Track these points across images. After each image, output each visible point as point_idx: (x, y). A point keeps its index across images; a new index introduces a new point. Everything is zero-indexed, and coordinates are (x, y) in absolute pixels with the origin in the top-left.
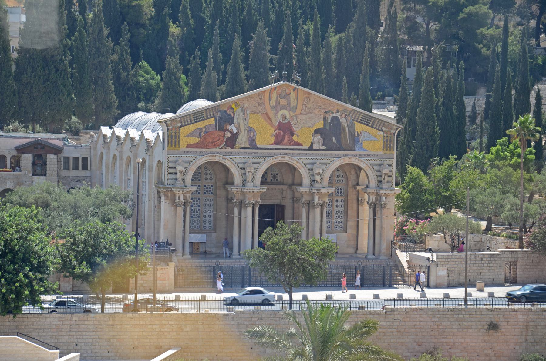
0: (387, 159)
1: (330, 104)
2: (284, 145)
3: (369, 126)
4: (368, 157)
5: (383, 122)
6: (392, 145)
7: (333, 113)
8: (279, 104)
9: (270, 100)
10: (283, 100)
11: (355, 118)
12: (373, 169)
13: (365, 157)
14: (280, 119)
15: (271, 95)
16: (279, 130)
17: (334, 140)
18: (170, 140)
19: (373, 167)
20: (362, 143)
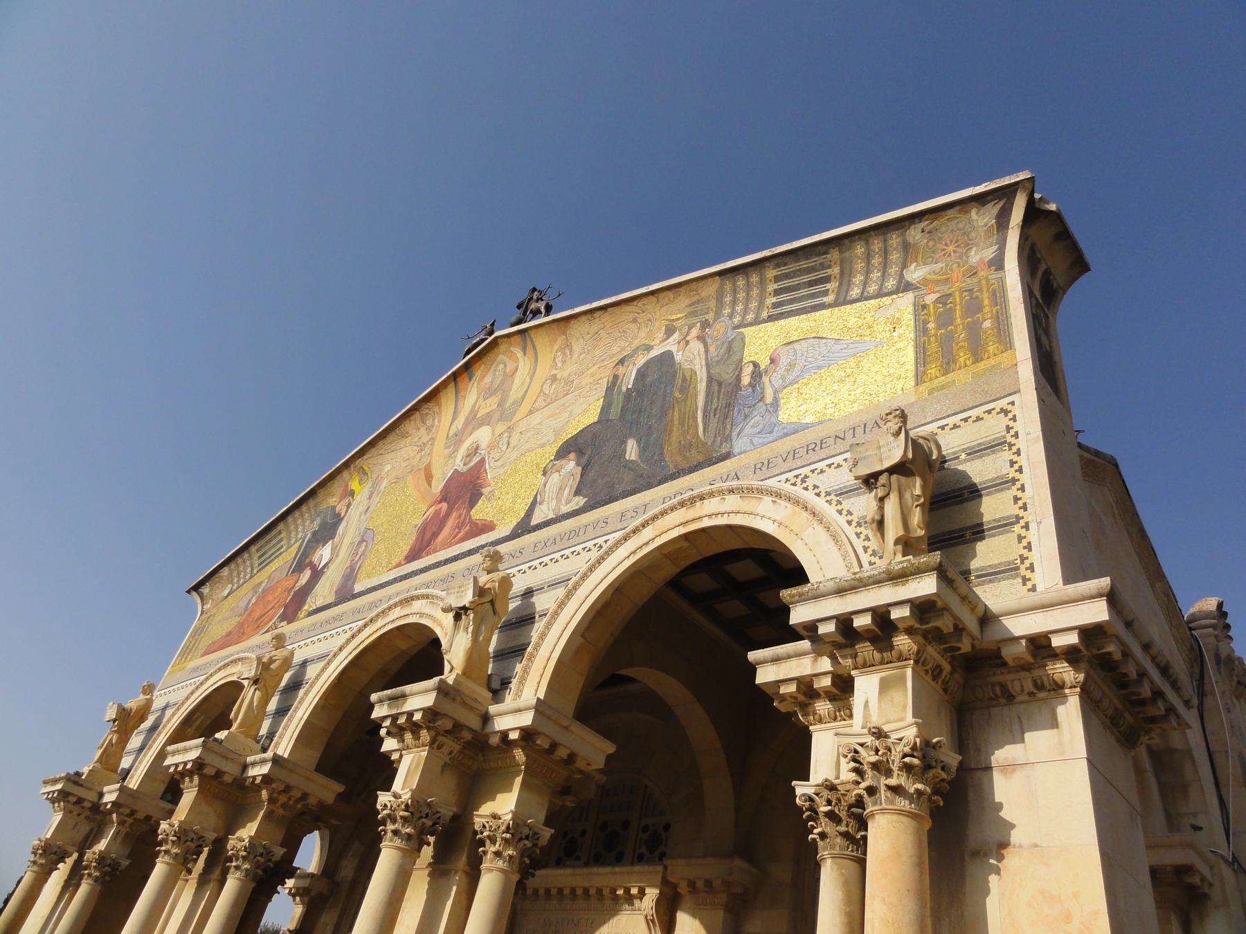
0: (955, 419)
1: (635, 321)
2: (435, 551)
3: (823, 306)
4: (813, 457)
5: (894, 239)
6: (987, 324)
7: (652, 348)
8: (475, 416)
9: (454, 419)
10: (490, 400)
11: (745, 311)
12: (842, 520)
13: (790, 464)
14: (459, 464)
15: (460, 403)
16: (440, 502)
17: (632, 450)
18: (188, 644)
19: (847, 504)
20: (776, 404)
